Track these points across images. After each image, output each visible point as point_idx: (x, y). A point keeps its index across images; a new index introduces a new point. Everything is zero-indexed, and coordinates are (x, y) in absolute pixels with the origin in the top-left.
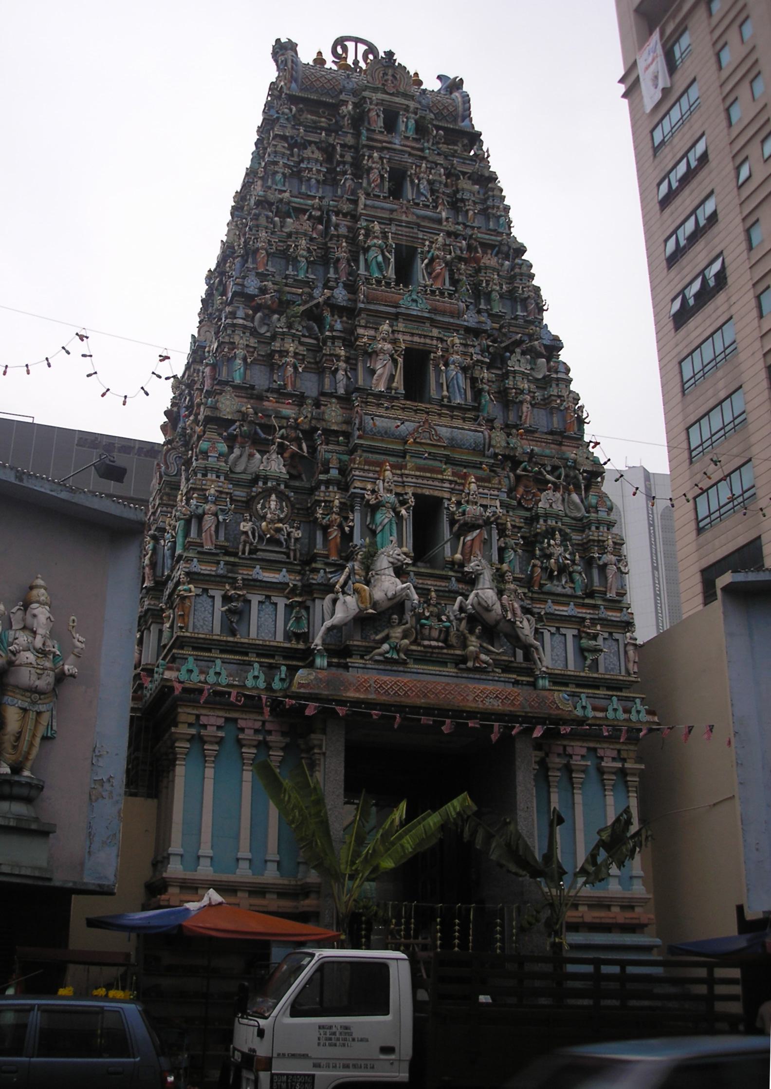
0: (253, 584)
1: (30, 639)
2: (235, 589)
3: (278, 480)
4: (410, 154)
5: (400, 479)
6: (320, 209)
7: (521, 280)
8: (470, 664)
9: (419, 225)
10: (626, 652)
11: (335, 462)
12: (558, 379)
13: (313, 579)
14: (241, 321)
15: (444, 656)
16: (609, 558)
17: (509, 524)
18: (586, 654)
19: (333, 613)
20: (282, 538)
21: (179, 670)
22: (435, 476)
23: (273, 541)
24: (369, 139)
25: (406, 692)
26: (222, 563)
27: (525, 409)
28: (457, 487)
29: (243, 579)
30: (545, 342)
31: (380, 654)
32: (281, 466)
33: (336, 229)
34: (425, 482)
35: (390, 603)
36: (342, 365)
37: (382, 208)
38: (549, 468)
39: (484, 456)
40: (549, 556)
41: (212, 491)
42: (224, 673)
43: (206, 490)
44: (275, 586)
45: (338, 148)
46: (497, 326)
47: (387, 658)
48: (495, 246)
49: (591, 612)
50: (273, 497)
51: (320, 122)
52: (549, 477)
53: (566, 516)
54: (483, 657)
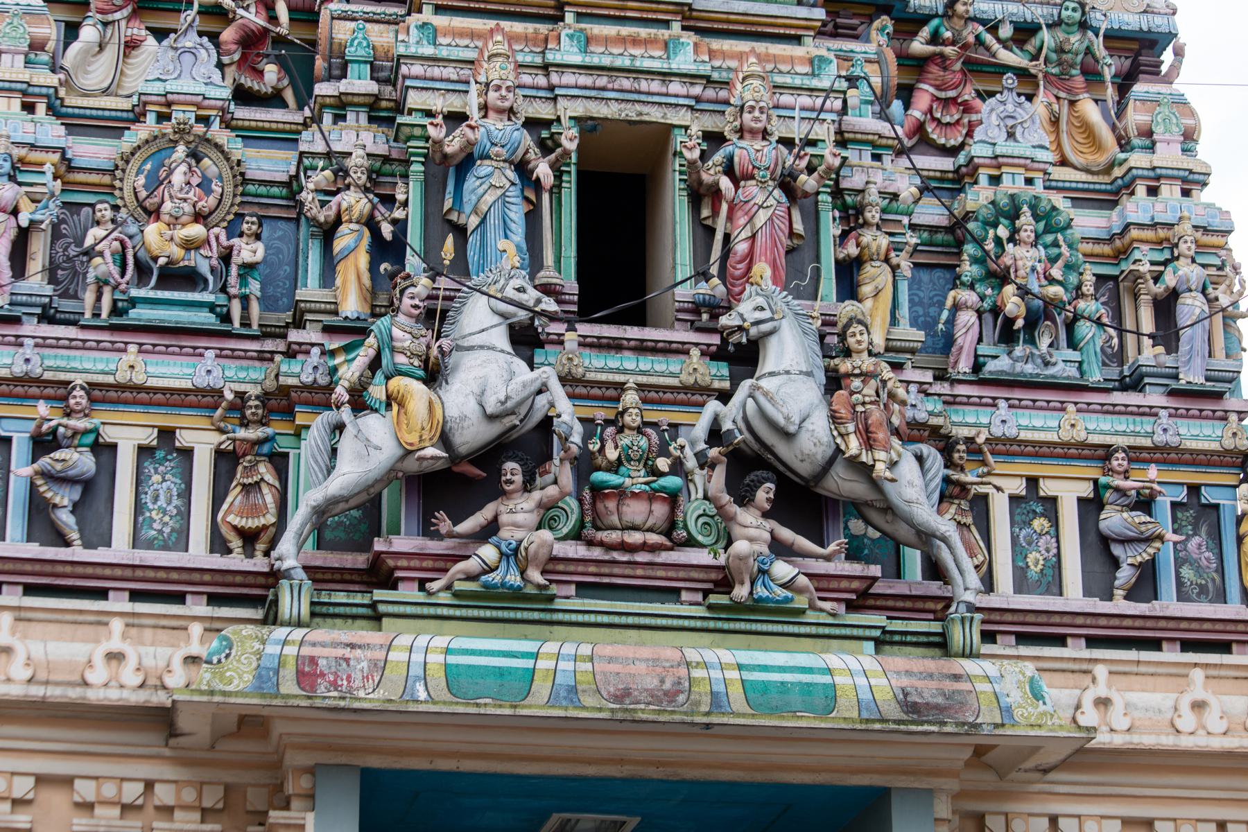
5: (542, 81)
8: (741, 592)
16: (1187, 272)
17: (873, 196)
19: (330, 470)
20: (204, 268)
28: (710, 93)
31: (471, 577)
35: (493, 430)
38: (1006, 31)
40: (1001, 278)
47: (486, 586)
53: (1064, 162)
54: (782, 569)
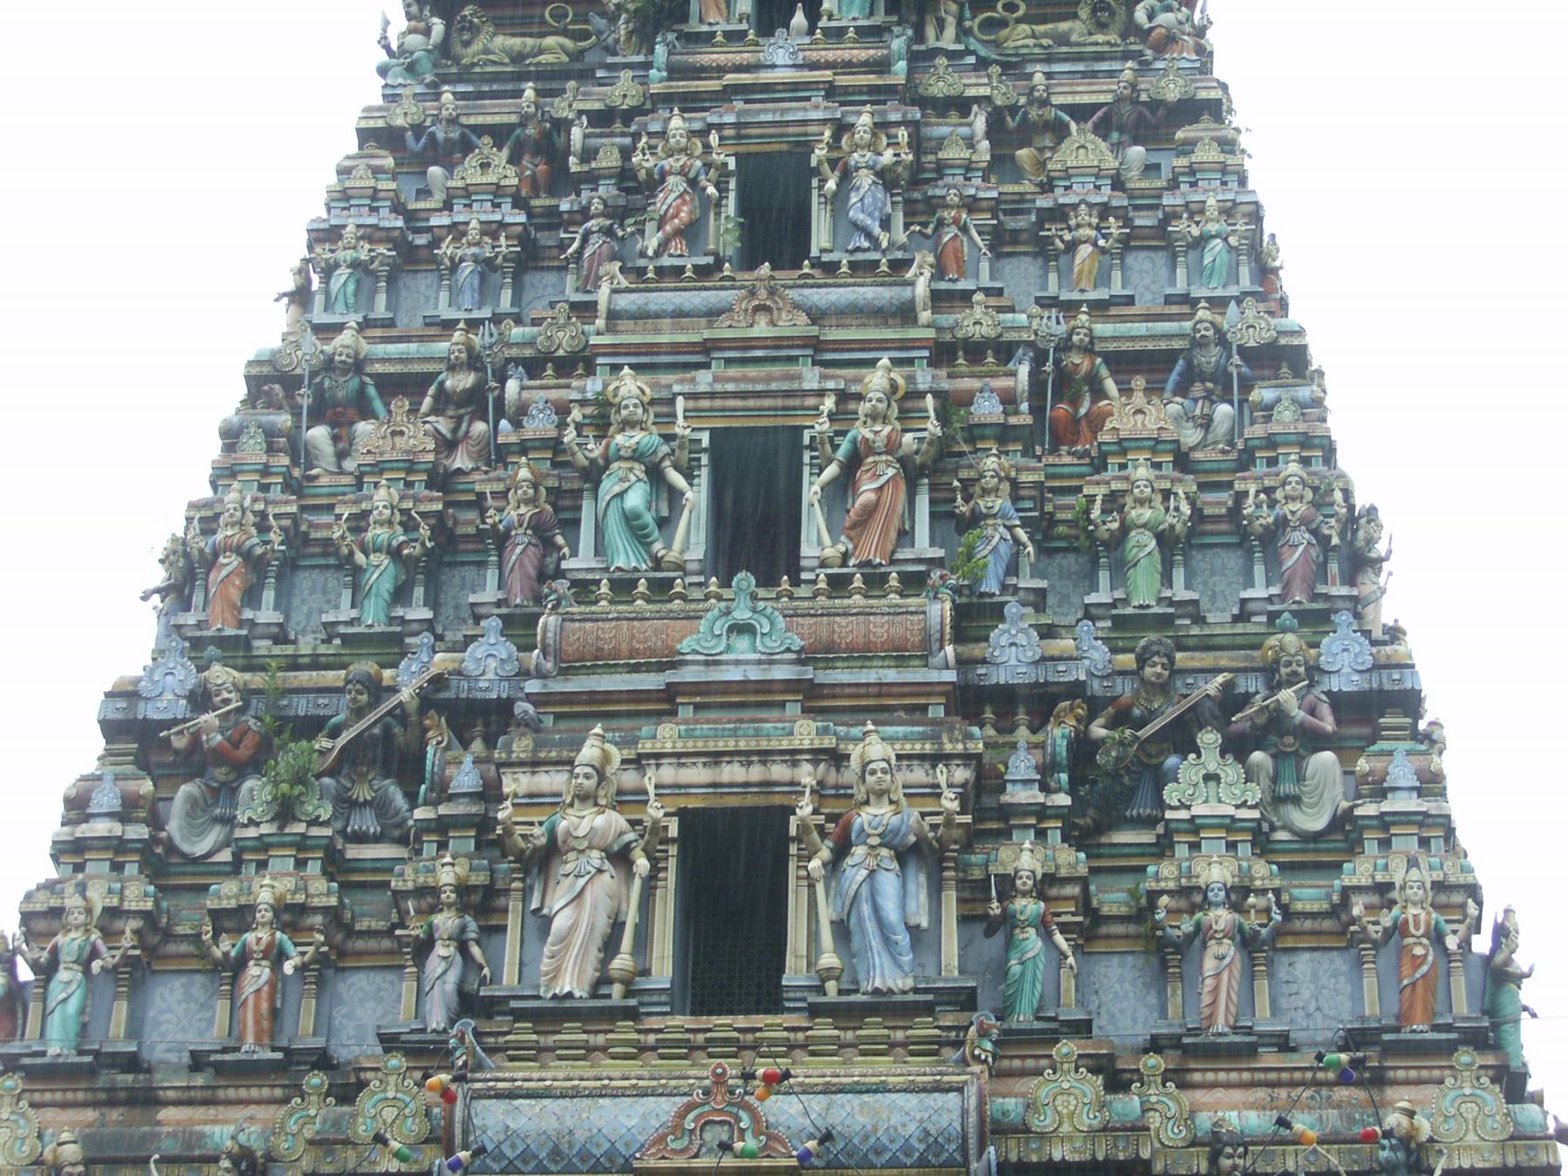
4: (831, 91)
6: (473, 361)
7: (1272, 462)
12: (1385, 822)
14: (101, 828)
24: (675, 72)
27: (1209, 965)
30: (1335, 684)
33: (517, 425)
36: (445, 921)
37: (679, 314)
45: (576, 134)
46: (1127, 660)
48: (1170, 357)
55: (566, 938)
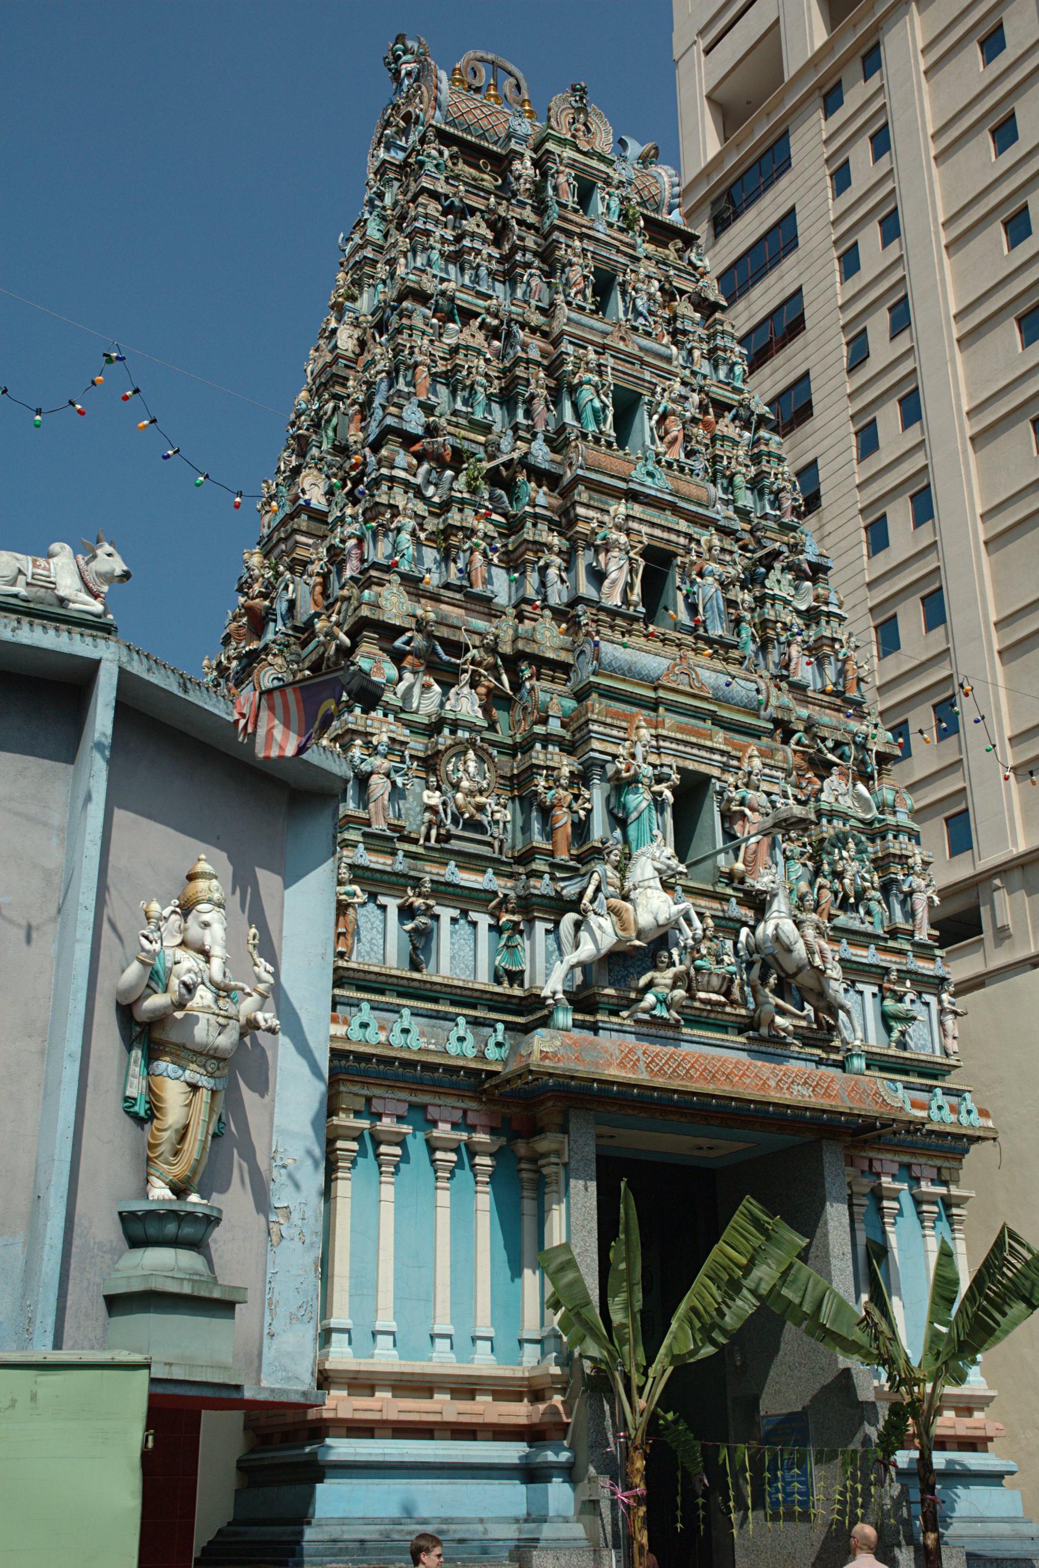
0: (445, 892)
1: (202, 965)
2: (419, 895)
3: (471, 727)
8: (764, 1031)
9: (643, 363)
10: (941, 1023)
11: (556, 708)
13: (535, 887)
15: (726, 1017)
18: (893, 1023)
19: (577, 946)
21: (346, 1022)
22: (702, 742)
23: (477, 826)
25: (688, 1072)
26: (401, 853)
29: (432, 881)
32: (476, 708)
34: (688, 750)
37: (591, 328)
38: (830, 744)
39: (758, 717)
41: (384, 738)
42: (415, 1030)
43: (372, 735)
44: (474, 894)
47: (652, 1016)
49: (898, 960)
50: (471, 754)
51: (482, 180)
52: (830, 756)
54: (779, 1020)
55: (614, 582)
